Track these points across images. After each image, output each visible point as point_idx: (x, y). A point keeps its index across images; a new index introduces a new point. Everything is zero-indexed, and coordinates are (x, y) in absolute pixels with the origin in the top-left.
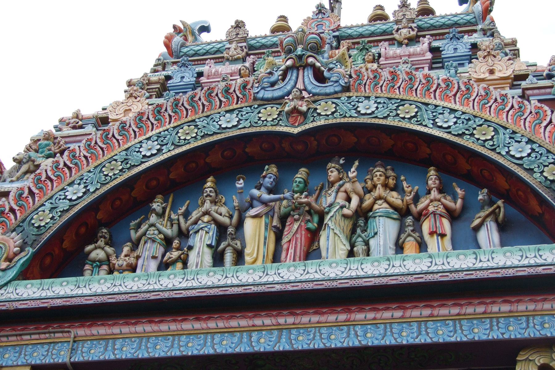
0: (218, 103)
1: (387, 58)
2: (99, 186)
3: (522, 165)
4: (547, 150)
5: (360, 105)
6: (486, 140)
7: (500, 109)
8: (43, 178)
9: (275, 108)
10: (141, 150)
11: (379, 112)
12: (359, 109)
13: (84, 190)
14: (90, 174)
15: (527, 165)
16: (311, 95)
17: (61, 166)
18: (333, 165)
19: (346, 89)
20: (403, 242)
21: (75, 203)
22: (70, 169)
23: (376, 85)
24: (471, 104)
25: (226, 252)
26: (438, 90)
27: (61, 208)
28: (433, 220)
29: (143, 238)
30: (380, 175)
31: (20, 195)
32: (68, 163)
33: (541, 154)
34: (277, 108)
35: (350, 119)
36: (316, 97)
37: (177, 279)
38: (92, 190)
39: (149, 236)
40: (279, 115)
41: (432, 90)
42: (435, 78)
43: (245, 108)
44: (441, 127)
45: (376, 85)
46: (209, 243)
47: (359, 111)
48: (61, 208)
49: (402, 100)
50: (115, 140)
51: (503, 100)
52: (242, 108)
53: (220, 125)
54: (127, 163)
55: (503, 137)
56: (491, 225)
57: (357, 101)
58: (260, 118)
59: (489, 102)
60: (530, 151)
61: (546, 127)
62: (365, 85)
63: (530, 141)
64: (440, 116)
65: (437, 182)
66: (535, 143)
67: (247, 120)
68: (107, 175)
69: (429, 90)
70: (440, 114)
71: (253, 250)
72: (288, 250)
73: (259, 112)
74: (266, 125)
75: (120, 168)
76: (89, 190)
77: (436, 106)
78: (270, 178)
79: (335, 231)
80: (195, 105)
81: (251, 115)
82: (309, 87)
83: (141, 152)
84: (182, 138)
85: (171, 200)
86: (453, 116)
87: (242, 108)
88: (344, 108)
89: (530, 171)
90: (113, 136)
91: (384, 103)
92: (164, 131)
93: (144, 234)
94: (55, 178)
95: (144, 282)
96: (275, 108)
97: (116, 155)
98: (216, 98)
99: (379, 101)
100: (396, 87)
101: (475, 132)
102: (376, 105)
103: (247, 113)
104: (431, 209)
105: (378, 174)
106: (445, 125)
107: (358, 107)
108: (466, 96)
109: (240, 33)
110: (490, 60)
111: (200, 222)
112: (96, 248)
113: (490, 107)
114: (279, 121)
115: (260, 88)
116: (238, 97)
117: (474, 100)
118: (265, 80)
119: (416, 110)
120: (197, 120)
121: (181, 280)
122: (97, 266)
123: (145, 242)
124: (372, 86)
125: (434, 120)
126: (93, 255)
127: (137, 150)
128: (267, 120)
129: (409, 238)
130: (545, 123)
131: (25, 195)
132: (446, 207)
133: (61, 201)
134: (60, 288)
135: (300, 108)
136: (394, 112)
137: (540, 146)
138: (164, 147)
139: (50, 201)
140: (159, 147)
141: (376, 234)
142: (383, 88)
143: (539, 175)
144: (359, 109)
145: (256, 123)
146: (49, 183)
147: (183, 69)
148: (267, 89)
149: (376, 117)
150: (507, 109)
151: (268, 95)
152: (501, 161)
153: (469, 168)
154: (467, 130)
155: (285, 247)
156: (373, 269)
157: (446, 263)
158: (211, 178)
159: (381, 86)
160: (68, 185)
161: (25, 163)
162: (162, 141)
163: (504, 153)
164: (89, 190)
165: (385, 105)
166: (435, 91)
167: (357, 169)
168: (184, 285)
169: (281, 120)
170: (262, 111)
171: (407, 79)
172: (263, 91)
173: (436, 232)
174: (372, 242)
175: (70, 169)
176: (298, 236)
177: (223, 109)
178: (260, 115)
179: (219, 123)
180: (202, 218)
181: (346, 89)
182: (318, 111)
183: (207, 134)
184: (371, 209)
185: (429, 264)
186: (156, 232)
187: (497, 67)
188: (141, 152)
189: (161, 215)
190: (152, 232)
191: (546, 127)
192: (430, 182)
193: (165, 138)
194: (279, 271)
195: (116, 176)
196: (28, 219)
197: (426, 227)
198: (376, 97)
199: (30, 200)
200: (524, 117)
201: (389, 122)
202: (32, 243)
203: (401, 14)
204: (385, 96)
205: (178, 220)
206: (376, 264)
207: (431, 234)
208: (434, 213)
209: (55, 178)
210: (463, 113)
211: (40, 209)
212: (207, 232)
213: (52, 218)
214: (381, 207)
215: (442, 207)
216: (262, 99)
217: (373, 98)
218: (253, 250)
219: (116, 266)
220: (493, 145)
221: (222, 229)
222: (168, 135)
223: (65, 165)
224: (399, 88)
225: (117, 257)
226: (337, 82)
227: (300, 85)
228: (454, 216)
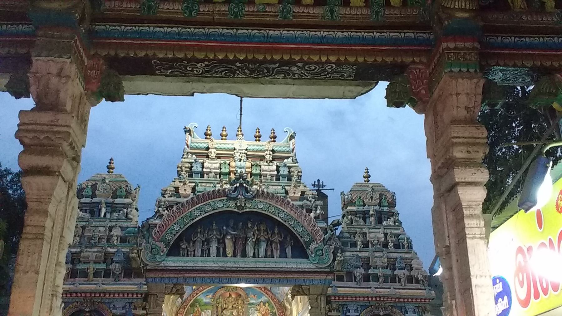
1: (263, 171)
63: (302, 226)
89: (301, 237)
152: (294, 232)
168: (214, 265)
197: (273, 245)
221: (219, 243)
227: (241, 193)
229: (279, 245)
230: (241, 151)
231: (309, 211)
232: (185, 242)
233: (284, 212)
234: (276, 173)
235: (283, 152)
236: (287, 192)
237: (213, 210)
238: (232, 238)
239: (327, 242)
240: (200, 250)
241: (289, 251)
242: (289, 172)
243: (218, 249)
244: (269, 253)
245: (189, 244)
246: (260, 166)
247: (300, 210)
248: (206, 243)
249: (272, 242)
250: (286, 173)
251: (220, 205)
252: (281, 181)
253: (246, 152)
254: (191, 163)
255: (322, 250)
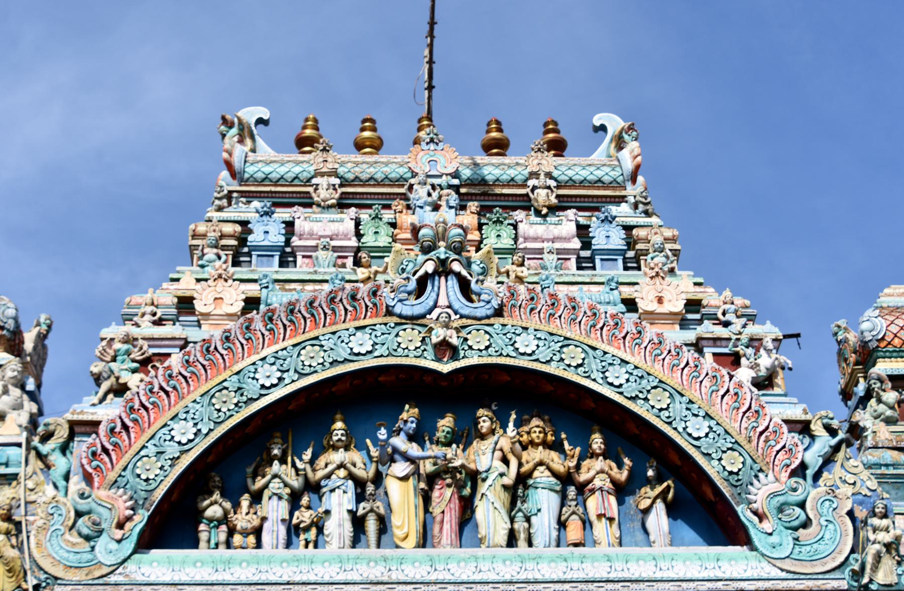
0: (343, 312)
1: (526, 239)
2: (212, 426)
3: (699, 447)
4: (726, 431)
5: (518, 339)
6: (661, 410)
7: (674, 365)
8: (137, 406)
9: (416, 332)
10: (257, 376)
11: (541, 353)
12: (517, 345)
13: (194, 430)
14: (198, 406)
15: (705, 448)
16: (458, 316)
17: (156, 389)
18: (486, 413)
19: (499, 313)
20: (567, 520)
21: (186, 447)
22: (167, 393)
23: (532, 310)
24: (642, 354)
25: (368, 518)
26: (605, 328)
27: (170, 454)
28: (600, 498)
29: (266, 491)
30: (540, 432)
31: (112, 430)
32: (164, 385)
33: (719, 435)
34: (420, 332)
35: (508, 358)
36: (464, 320)
37: (332, 567)
38: (204, 431)
39: (275, 491)
40: (422, 341)
41: (598, 327)
42: (602, 311)
43: (378, 326)
44: (611, 384)
45: (532, 310)
46: (350, 508)
47: (517, 349)
48: (170, 454)
49: (566, 338)
50: (218, 355)
51: (678, 354)
52: (375, 325)
53: (351, 349)
54: (242, 395)
55: (678, 408)
56: (660, 506)
57: (514, 333)
58: (400, 344)
59: (662, 353)
60: (707, 430)
61: (723, 396)
62: (520, 307)
63: (707, 416)
64: (611, 368)
65: (603, 446)
66: (712, 418)
67: (383, 344)
68: (219, 411)
69: (594, 326)
70: (610, 364)
71: (403, 522)
72: (442, 522)
73: (397, 335)
74: (407, 356)
75: (235, 401)
76: (199, 430)
77: (605, 353)
78: (412, 422)
79: (495, 505)
80: (315, 313)
81: (387, 338)
82: (456, 306)
83: (257, 380)
84: (307, 363)
85: (290, 438)
86: (624, 370)
87: (375, 325)
88: (500, 341)
90: (216, 348)
91: (545, 339)
92: (282, 350)
93: (266, 486)
94: (150, 407)
95: (295, 569)
96: (416, 332)
97: (226, 380)
98: (341, 305)
99: (538, 336)
100: (556, 316)
101: (649, 396)
102: (536, 342)
103: (383, 334)
104: (597, 483)
105: (538, 430)
106: (616, 383)
107: (515, 342)
108: (637, 341)
109: (329, 160)
110: (658, 283)
111: (334, 477)
112: (211, 504)
113: (664, 360)
114: (423, 351)
115: (396, 300)
116: (367, 306)
117: (646, 348)
118: (402, 289)
119: (583, 356)
120: (321, 338)
121: (338, 570)
122: (214, 527)
123: (270, 498)
124: (528, 310)
125: (603, 373)
126: (209, 513)
127: (252, 375)
128: (409, 349)
129: (574, 517)
130: (722, 392)
131: (118, 430)
132: (613, 481)
133: (167, 443)
134: (195, 570)
135: (450, 340)
136: (558, 354)
137: (718, 424)
138: (285, 375)
139: (152, 442)
140: (279, 374)
141: (539, 510)
142: (542, 314)
143: (717, 462)
144: (517, 345)
145: (395, 350)
146: (144, 413)
147: (264, 218)
148: (405, 302)
149: (537, 360)
150: (682, 365)
151: (407, 311)
153: (637, 432)
154: (641, 392)
155: (438, 519)
156: (550, 571)
157: (625, 569)
158: (338, 416)
159: (539, 312)
160: (172, 419)
161: (106, 379)
162: (281, 365)
163: (681, 430)
164: (199, 430)
165: (546, 343)
166: (602, 328)
167: (515, 426)
169: (425, 350)
170: (401, 333)
171: (570, 307)
172: (399, 304)
173: (604, 515)
174: (534, 519)
175: (167, 393)
176: (452, 506)
177: (352, 325)
178: (399, 340)
179: (350, 345)
180: (337, 472)
181: (499, 313)
182: (470, 343)
183: (336, 361)
184: (530, 474)
185: (609, 570)
186: (282, 485)
187: (666, 296)
188: (257, 380)
189: (283, 461)
190: (277, 485)
191: (723, 396)
192: (595, 446)
193: (285, 360)
194: (449, 567)
195: (231, 413)
196: (130, 466)
198: (536, 330)
199: (124, 434)
200: (700, 379)
201: (552, 369)
202: (144, 503)
203: (536, 162)
204: (546, 329)
205: (304, 470)
206: (553, 565)
207: (600, 516)
208: (601, 489)
209: (150, 407)
210: (636, 367)
211: (142, 453)
212: (345, 492)
213: (161, 468)
214: (542, 476)
215: (608, 480)
216: (400, 316)
217: (531, 331)
218: (403, 522)
219: (238, 527)
220: (669, 417)
222: (287, 357)
223: (162, 388)
224: (560, 317)
225: (235, 513)
226: (488, 302)
227: (443, 301)
228: (622, 491)
229: (613, 500)
230: (436, 181)
231: (735, 360)
232: (216, 496)
233: (624, 362)
234: (576, 244)
235: (599, 183)
236: (630, 305)
237: (334, 363)
238: (416, 473)
239: (817, 476)
240: (283, 530)
241: (659, 520)
242: (631, 243)
243: (358, 523)
244: (574, 531)
245: (236, 506)
246: (515, 227)
247: (689, 355)
248: (305, 500)
249: (583, 489)
250: (617, 239)
251: (362, 342)
252: (599, 271)
253: (456, 182)
254: (244, 224)
255: (802, 505)
